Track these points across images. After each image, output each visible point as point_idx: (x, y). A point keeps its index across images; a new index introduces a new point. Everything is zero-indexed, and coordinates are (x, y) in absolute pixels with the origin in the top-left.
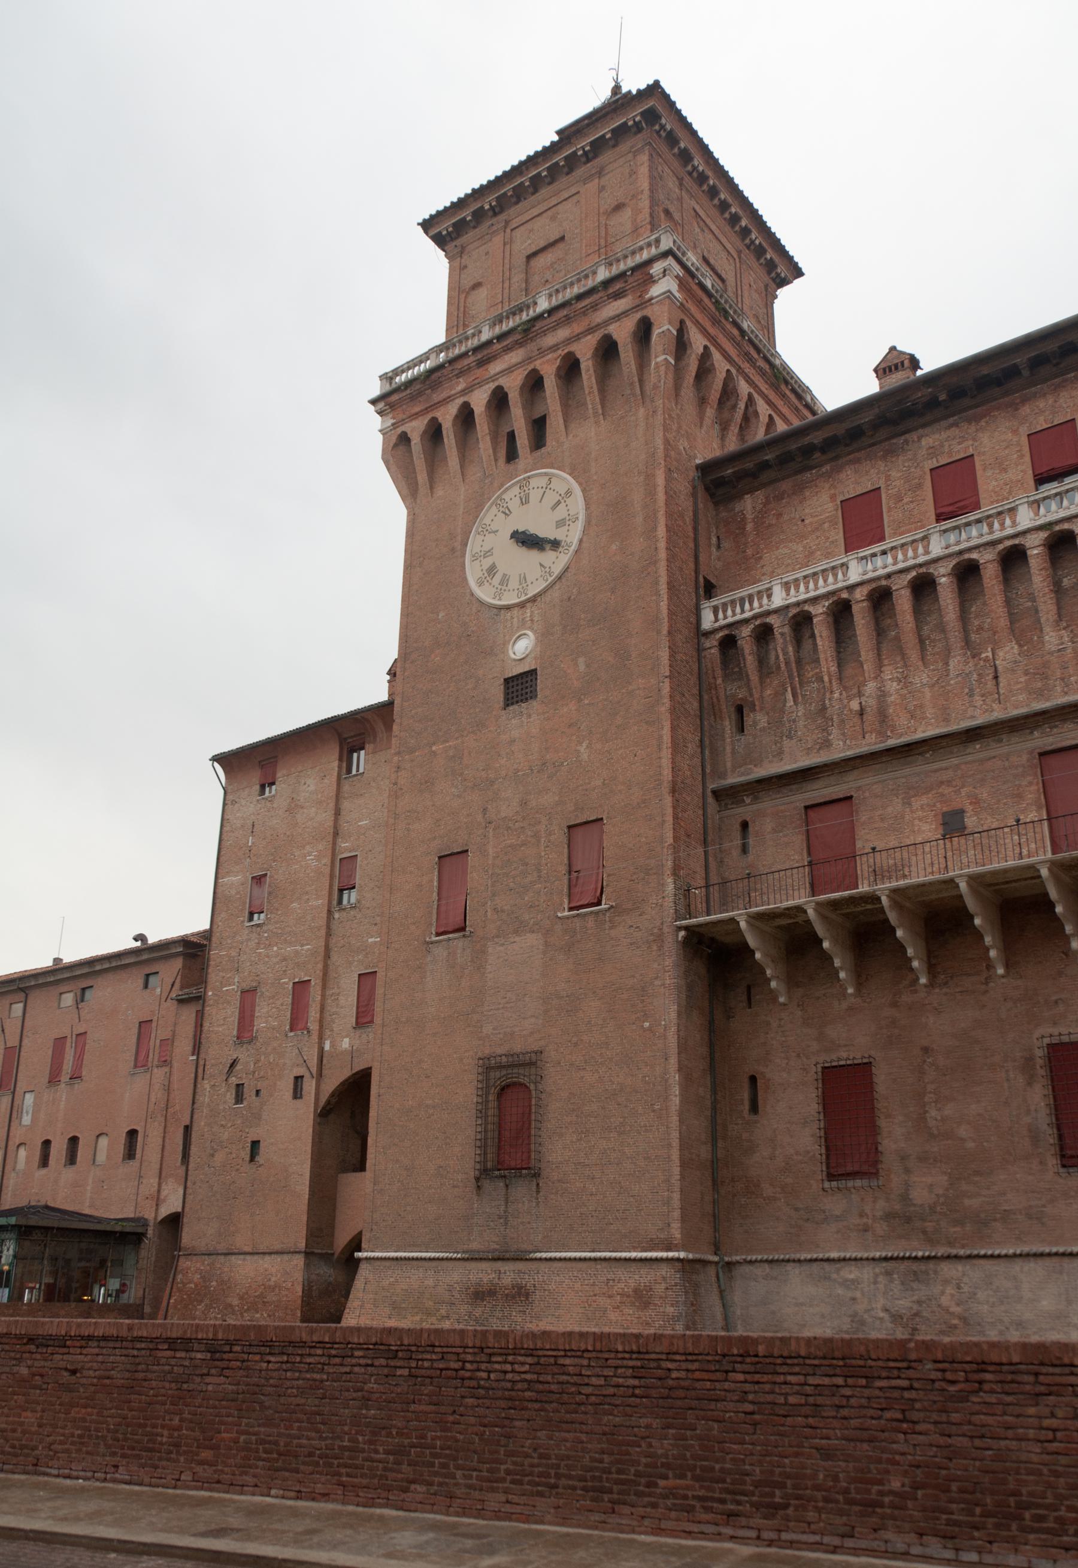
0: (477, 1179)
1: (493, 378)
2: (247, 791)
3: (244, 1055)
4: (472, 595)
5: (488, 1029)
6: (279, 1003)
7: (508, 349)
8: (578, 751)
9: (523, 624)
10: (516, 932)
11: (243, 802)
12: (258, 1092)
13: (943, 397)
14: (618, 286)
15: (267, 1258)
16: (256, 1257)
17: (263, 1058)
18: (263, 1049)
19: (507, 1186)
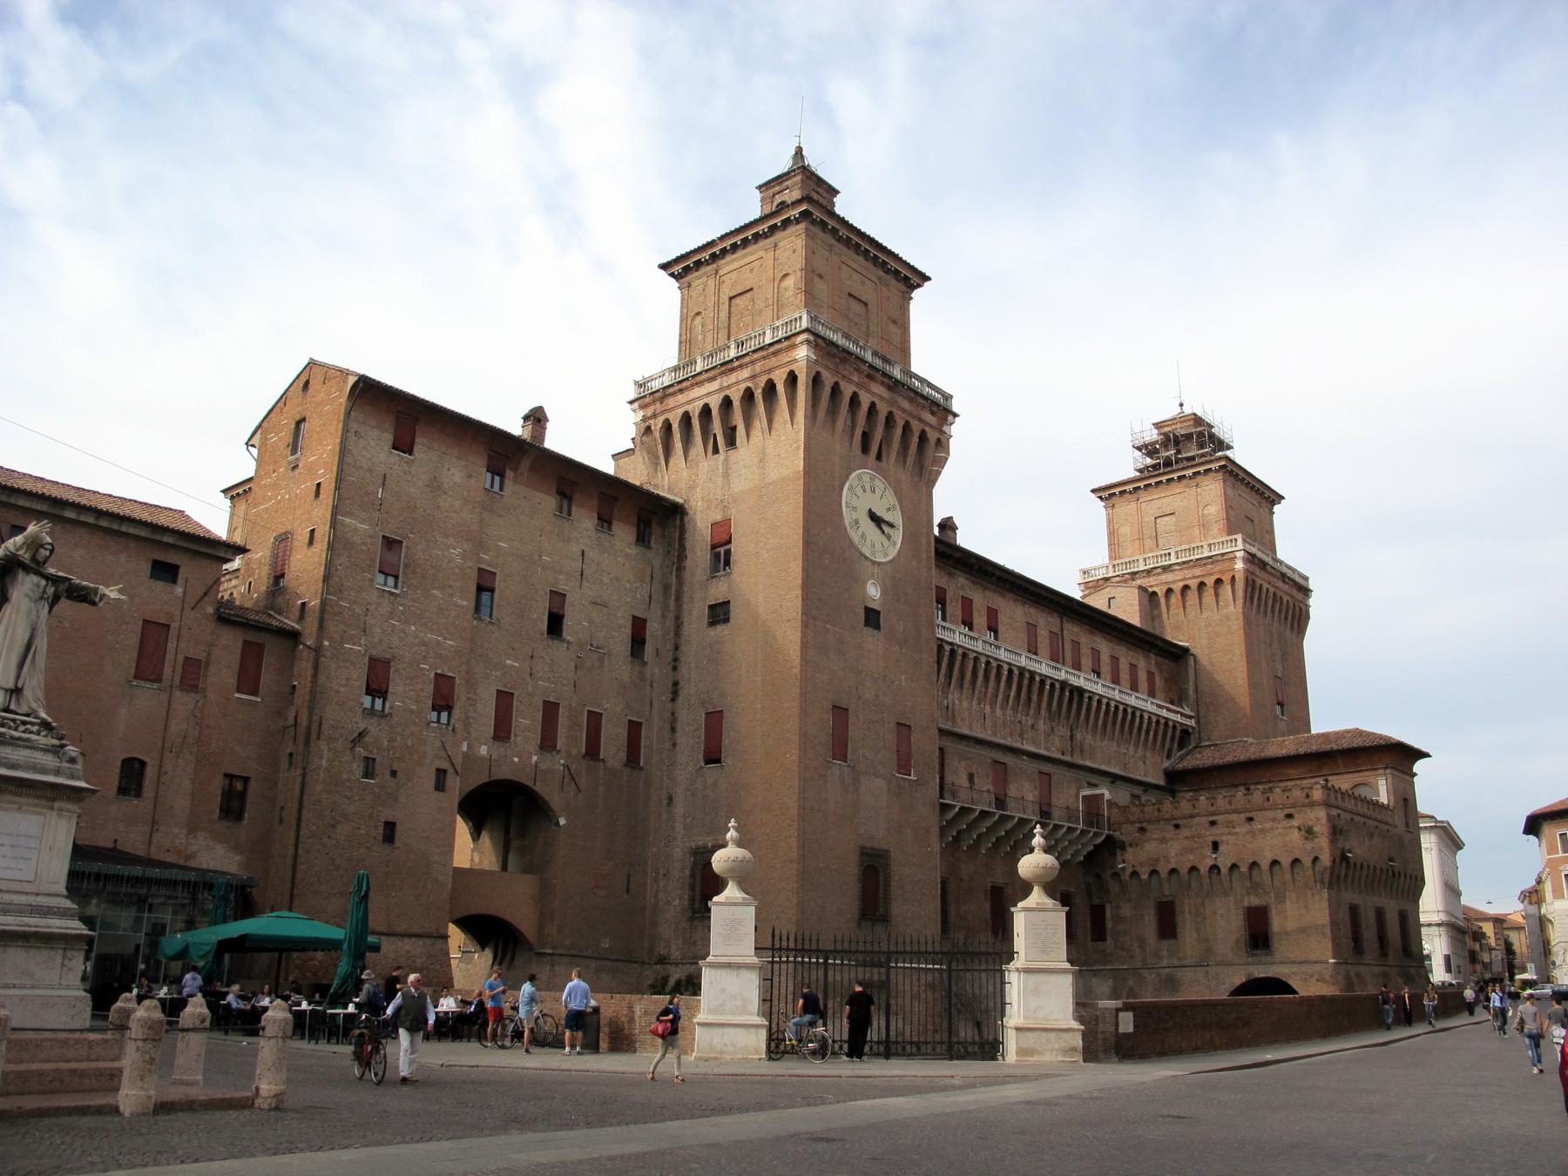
0: (859, 919)
1: (873, 394)
2: (376, 432)
3: (373, 727)
4: (846, 530)
5: (862, 830)
6: (419, 687)
7: (883, 384)
8: (900, 680)
9: (872, 577)
10: (874, 774)
11: (372, 444)
12: (394, 773)
13: (976, 568)
14: (935, 409)
15: (406, 940)
16: (393, 939)
17: (399, 738)
18: (399, 729)
19: (873, 925)
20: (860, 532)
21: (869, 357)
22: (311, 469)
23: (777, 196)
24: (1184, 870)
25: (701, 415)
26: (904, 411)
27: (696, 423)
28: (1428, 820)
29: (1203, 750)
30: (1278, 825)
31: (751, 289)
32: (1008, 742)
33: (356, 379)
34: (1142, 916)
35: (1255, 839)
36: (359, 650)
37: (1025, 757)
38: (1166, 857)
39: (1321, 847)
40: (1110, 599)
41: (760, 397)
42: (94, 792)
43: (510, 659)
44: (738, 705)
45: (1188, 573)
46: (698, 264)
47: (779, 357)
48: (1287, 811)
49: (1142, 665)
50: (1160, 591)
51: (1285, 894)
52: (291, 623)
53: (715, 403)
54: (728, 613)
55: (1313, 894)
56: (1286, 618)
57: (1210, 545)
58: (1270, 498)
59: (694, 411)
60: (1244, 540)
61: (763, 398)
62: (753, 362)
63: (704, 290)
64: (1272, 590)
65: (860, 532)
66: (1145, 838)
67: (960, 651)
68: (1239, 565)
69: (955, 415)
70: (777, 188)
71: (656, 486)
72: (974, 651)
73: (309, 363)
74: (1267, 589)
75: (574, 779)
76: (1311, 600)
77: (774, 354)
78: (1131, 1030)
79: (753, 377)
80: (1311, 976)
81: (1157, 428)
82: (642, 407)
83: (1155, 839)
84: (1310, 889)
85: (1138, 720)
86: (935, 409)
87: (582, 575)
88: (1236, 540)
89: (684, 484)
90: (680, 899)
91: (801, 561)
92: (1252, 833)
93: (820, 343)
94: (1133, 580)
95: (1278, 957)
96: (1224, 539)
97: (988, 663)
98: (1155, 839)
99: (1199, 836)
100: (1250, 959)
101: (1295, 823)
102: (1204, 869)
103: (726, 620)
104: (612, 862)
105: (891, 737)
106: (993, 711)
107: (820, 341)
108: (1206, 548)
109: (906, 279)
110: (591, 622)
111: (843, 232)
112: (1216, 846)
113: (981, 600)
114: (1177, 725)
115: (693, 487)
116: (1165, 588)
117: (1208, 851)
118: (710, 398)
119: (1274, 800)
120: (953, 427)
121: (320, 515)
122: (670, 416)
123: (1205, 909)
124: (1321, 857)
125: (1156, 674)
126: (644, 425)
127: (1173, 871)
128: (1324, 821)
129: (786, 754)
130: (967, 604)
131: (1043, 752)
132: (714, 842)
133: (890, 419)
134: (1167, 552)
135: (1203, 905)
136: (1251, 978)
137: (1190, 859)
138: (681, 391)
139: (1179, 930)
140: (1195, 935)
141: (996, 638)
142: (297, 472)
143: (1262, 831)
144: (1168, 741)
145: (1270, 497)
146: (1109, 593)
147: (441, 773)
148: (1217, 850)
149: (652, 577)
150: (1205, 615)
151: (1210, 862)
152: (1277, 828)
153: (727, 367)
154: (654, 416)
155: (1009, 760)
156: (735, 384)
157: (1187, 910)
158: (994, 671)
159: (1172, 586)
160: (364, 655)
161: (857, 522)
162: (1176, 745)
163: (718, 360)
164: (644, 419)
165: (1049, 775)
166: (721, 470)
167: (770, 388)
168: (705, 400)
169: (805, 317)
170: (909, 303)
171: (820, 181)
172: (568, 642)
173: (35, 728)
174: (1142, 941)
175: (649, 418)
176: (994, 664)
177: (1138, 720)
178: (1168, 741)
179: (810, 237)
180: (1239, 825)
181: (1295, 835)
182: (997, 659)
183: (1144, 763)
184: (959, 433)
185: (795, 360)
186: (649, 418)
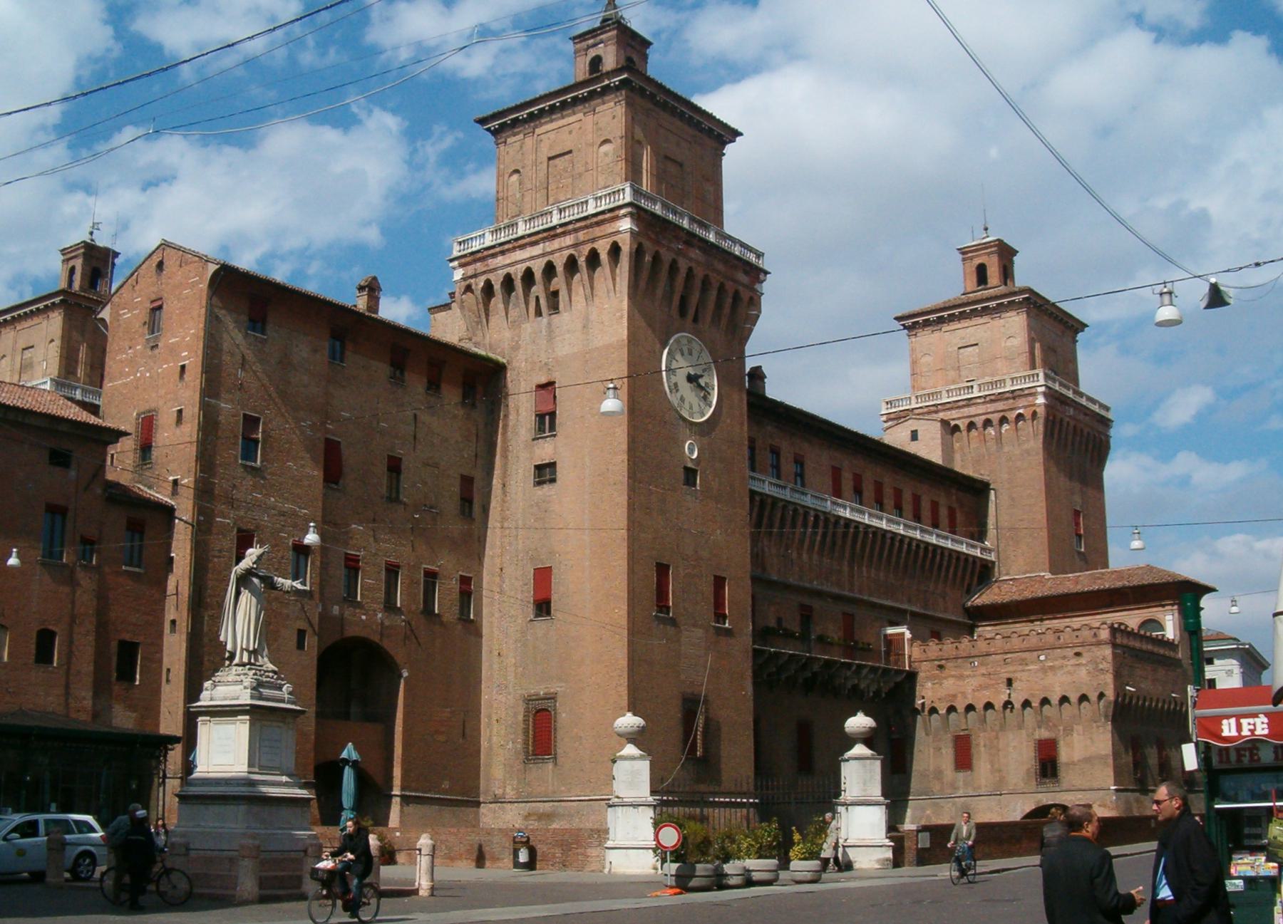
1: (691, 259)
5: (683, 677)
7: (700, 248)
20: (679, 395)
21: (685, 223)
22: (174, 350)
23: (591, 50)
24: (979, 706)
25: (523, 278)
26: (719, 272)
27: (518, 284)
28: (1231, 641)
29: (1001, 584)
30: (1068, 663)
31: (570, 152)
32: (816, 584)
33: (217, 267)
36: (228, 523)
37: (829, 600)
38: (963, 693)
39: (1106, 683)
40: (912, 432)
41: (584, 265)
42: (302, 712)
43: (355, 524)
44: (566, 563)
45: (991, 407)
46: (516, 122)
47: (602, 227)
48: (1077, 650)
49: (943, 501)
50: (962, 424)
52: (163, 497)
53: (538, 267)
54: (554, 472)
55: (1098, 727)
56: (1086, 450)
57: (1012, 379)
58: (1072, 326)
59: (516, 274)
60: (1047, 377)
61: (587, 266)
62: (576, 230)
63: (521, 147)
64: (1072, 423)
65: (679, 395)
66: (943, 675)
67: (769, 501)
68: (1041, 400)
69: (766, 273)
70: (591, 42)
71: (477, 344)
72: (782, 500)
73: (162, 244)
74: (1068, 423)
76: (1111, 430)
77: (598, 224)
78: (928, 845)
79: (575, 246)
81: (963, 253)
82: (462, 266)
83: (953, 676)
84: (1095, 722)
85: (938, 557)
86: (748, 268)
87: (415, 438)
88: (1038, 375)
89: (506, 344)
91: (626, 427)
92: (1044, 670)
93: (639, 214)
94: (936, 412)
95: (1065, 785)
96: (1026, 373)
97: (795, 511)
98: (953, 676)
100: (1040, 790)
101: (1083, 660)
102: (998, 705)
103: (553, 481)
105: (708, 589)
106: (800, 555)
107: (642, 213)
108: (1009, 382)
109: (720, 136)
110: (425, 483)
111: (660, 97)
112: (1010, 682)
113: (787, 448)
114: (977, 560)
115: (516, 348)
116: (967, 421)
117: (1003, 687)
118: (532, 262)
120: (764, 284)
121: (189, 396)
122: (491, 277)
124: (1106, 693)
125: (958, 511)
126: (464, 284)
127: (970, 708)
128: (1110, 658)
129: (614, 609)
130: (775, 452)
131: (846, 593)
132: (546, 690)
133: (706, 282)
134: (969, 384)
135: (997, 738)
136: (1041, 805)
137: (986, 696)
138: (503, 253)
139: (975, 761)
140: (989, 766)
141: (803, 485)
142: (156, 351)
144: (967, 577)
145: (1073, 326)
146: (910, 425)
147: (301, 634)
149: (477, 435)
150: (1006, 449)
151: (1005, 698)
152: (1067, 666)
153: (551, 233)
154: (475, 276)
155: (816, 604)
156: (559, 251)
157: (982, 744)
158: (801, 518)
159: (973, 419)
160: (233, 527)
161: (676, 385)
162: (975, 579)
163: (539, 225)
164: (464, 279)
165: (852, 615)
166: (544, 333)
167: (593, 259)
168: (528, 264)
169: (628, 190)
170: (721, 160)
171: (634, 35)
172: (405, 504)
173: (271, 674)
174: (939, 774)
175: (471, 277)
176: (801, 511)
177: (938, 557)
178: (967, 577)
179: (630, 104)
180: (1032, 662)
181: (1083, 672)
182: (804, 507)
183: (944, 598)
184: (768, 288)
185: (618, 232)
186: (471, 277)
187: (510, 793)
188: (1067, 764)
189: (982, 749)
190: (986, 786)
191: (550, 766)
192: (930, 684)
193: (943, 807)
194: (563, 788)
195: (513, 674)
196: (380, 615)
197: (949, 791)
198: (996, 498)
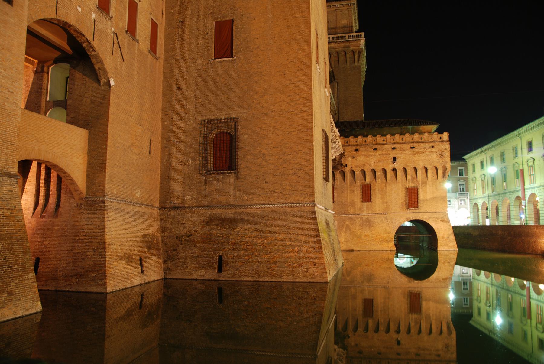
34: (354, 191)
35: (414, 157)
44: (248, 15)
51: (426, 182)
75: (120, 48)
80: (438, 219)
90: (192, 160)
95: (422, 211)
99: (387, 154)
100: (408, 211)
101: (434, 150)
104: (141, 127)
112: (395, 159)
119: (424, 139)
123: (386, 188)
132: (227, 116)
135: (386, 186)
139: (373, 198)
140: (381, 201)
143: (418, 152)
148: (396, 161)
152: (426, 152)
157: (377, 189)
174: (353, 204)
180: (407, 150)
181: (434, 156)
187: (189, 201)
188: (423, 200)
189: (377, 192)
190: (379, 210)
191: (232, 178)
192: (350, 158)
193: (355, 220)
194: (245, 198)
195: (193, 104)
196: (94, 16)
197: (358, 213)
198: (338, 86)
